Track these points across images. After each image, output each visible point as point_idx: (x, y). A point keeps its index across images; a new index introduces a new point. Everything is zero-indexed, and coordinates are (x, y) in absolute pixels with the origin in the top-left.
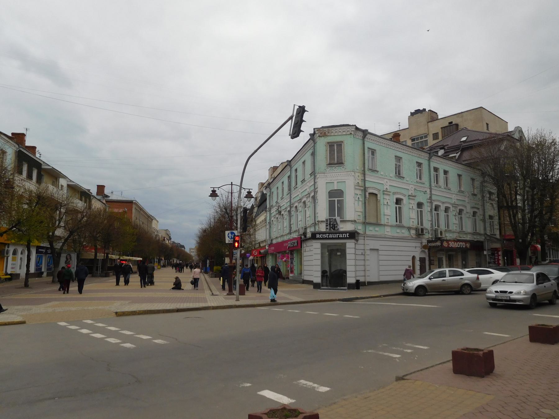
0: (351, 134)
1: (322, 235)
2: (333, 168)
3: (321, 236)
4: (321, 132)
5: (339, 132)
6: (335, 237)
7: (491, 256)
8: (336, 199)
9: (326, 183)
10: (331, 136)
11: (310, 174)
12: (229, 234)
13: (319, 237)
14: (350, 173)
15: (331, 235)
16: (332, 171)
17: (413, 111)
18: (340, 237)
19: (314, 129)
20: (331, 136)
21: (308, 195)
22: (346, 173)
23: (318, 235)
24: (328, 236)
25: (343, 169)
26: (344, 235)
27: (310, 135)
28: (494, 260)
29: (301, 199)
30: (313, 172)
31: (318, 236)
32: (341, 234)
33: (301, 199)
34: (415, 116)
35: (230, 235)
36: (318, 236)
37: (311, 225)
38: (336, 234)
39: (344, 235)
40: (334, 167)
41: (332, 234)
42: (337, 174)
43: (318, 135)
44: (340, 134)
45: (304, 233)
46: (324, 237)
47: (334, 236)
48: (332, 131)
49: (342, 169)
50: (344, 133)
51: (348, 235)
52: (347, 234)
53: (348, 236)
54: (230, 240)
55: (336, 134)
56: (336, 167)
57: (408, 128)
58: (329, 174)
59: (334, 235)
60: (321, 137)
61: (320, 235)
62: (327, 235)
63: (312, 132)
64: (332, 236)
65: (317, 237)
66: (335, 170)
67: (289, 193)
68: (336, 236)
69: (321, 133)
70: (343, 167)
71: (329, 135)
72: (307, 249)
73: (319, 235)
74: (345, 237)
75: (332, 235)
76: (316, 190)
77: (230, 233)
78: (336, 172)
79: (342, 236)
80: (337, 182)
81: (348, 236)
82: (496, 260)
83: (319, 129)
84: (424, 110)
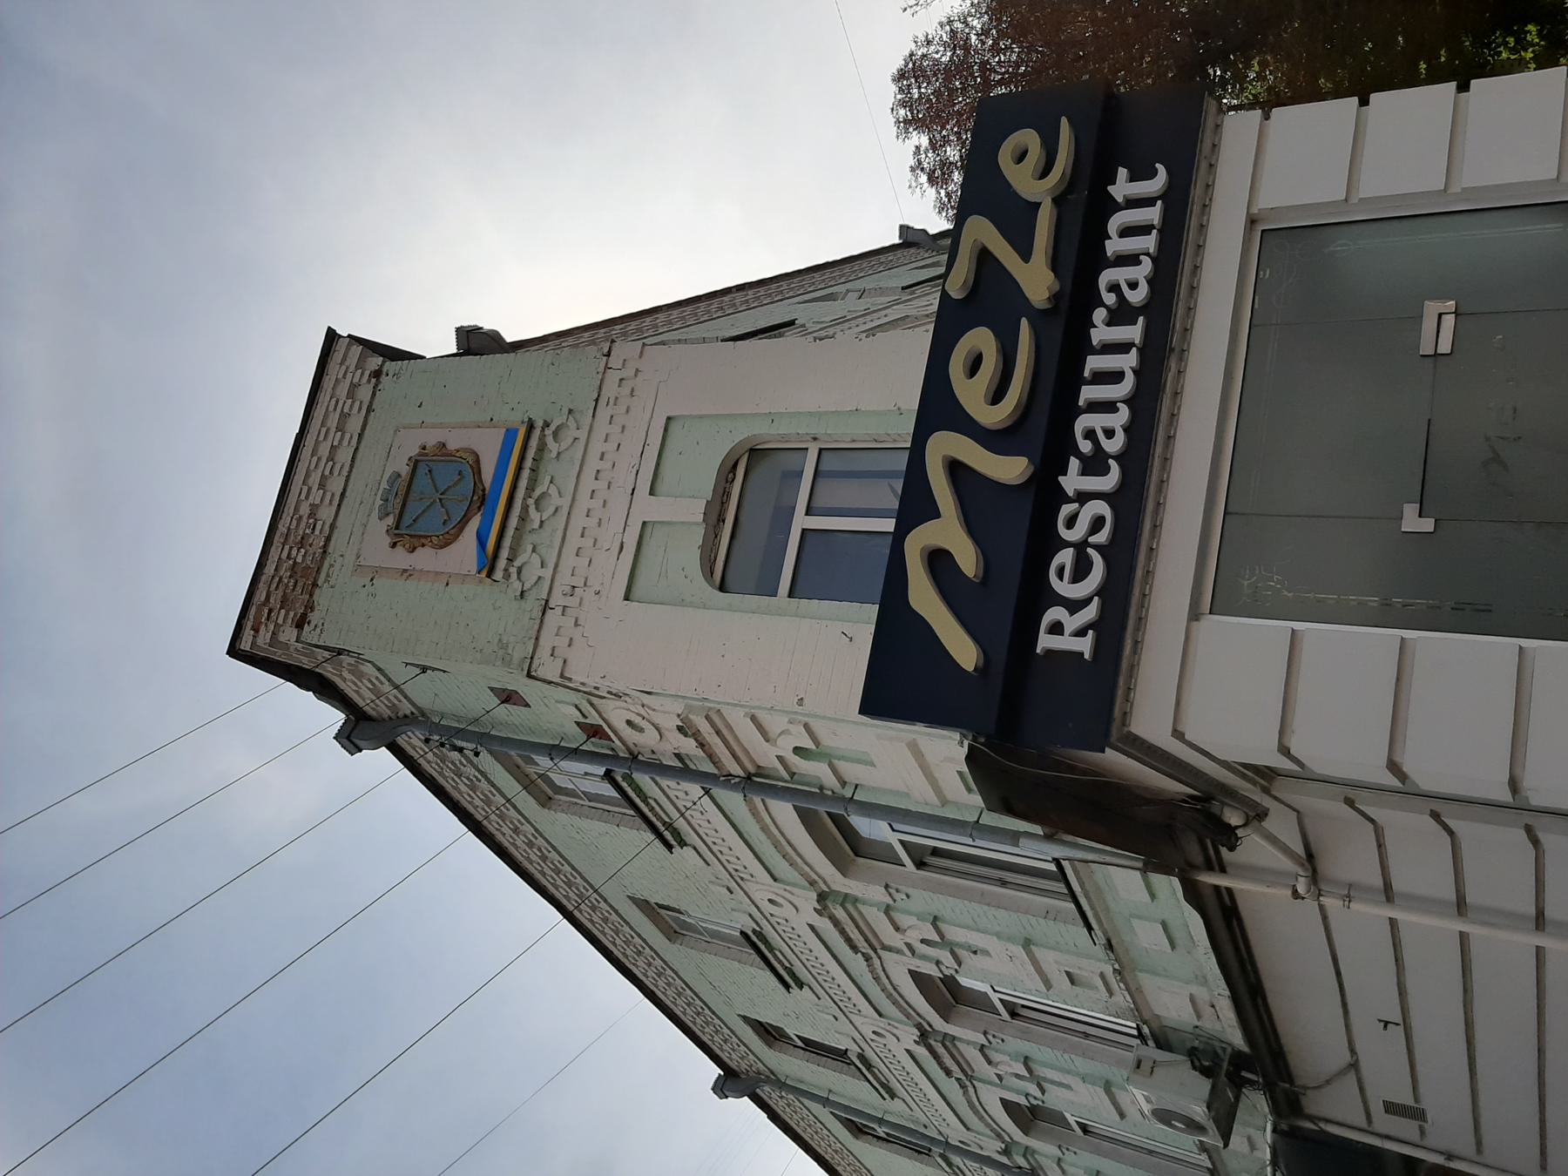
0: (377, 374)
1: (1065, 557)
2: (534, 515)
3: (1081, 571)
4: (275, 601)
5: (331, 458)
6: (1128, 362)
8: (801, 521)
9: (627, 598)
10: (332, 527)
11: (669, 847)
13: (1090, 613)
14: (612, 378)
15: (1083, 422)
16: (554, 531)
18: (1137, 297)
19: (234, 651)
20: (332, 527)
22: (604, 413)
24: (1095, 464)
26: (1126, 232)
27: (351, 739)
29: (919, 1027)
30: (608, 776)
31: (1072, 622)
36: (1072, 622)
37: (1101, 940)
38: (1077, 344)
39: (1126, 232)
40: (532, 509)
41: (1067, 409)
42: (588, 482)
43: (289, 635)
44: (344, 456)
45: (1206, 1072)
46: (1097, 524)
47: (1116, 377)
48: (305, 510)
49: (564, 445)
50: (354, 425)
51: (1133, 178)
52: (1122, 188)
53: (1156, 184)
55: (336, 485)
58: (569, 560)
59: (1103, 377)
60: (310, 607)
61: (1064, 588)
62: (1072, 481)
63: (335, 718)
64: (1109, 407)
65: (1085, 645)
66: (555, 500)
67: (941, 1156)
68: (1122, 348)
69: (284, 602)
70: (555, 434)
71: (322, 544)
72: (1388, 1081)
73: (1055, 613)
74: (1153, 214)
78: (565, 502)
79: (1132, 260)
80: (652, 493)
81: (1156, 184)
83: (253, 610)
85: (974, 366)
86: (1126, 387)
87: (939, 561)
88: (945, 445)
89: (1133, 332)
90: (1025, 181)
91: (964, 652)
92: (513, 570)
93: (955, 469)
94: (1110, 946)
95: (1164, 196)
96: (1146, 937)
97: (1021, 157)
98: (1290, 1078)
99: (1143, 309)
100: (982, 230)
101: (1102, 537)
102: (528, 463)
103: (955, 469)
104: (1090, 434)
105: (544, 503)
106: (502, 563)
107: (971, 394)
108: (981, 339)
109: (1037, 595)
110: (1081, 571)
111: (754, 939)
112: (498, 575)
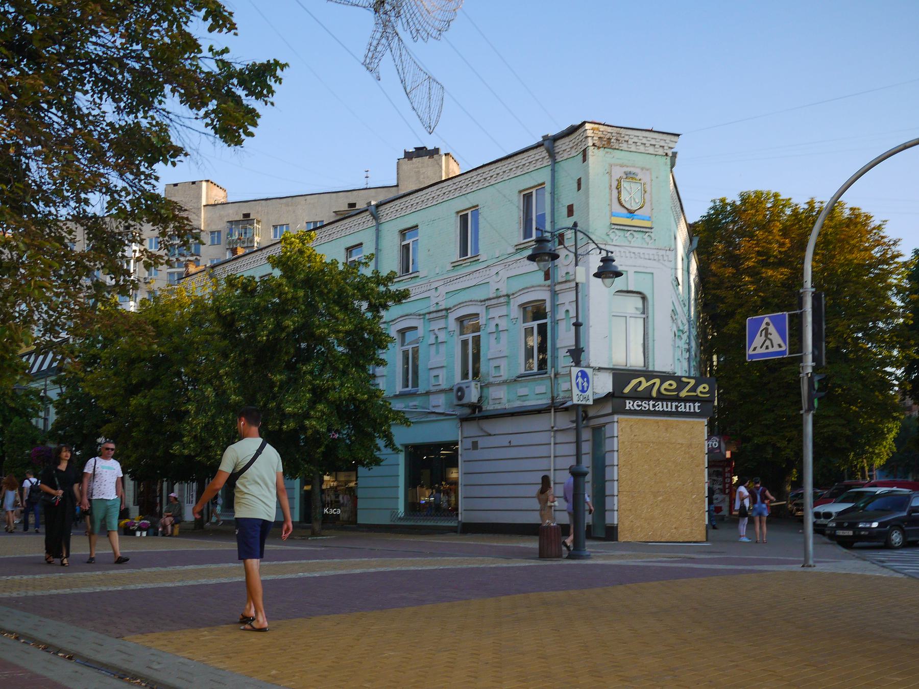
1: (640, 403)
3: (638, 406)
6: (669, 409)
7: (715, 478)
12: (577, 377)
13: (632, 408)
14: (663, 252)
15: (660, 403)
17: (411, 150)
18: (679, 409)
21: (502, 300)
22: (655, 252)
23: (630, 403)
24: (654, 406)
25: (650, 242)
26: (690, 406)
28: (721, 487)
29: (450, 309)
32: (683, 404)
33: (447, 310)
34: (414, 160)
35: (580, 380)
39: (690, 406)
40: (629, 232)
45: (478, 401)
46: (645, 408)
47: (667, 408)
52: (697, 404)
54: (580, 393)
56: (634, 233)
57: (397, 186)
59: (667, 405)
62: (651, 403)
64: (662, 407)
65: (627, 408)
68: (671, 408)
73: (632, 403)
75: (663, 405)
76: (558, 288)
77: (580, 374)
79: (685, 408)
81: (697, 411)
82: (727, 486)
84: (436, 151)
85: (671, 385)
86: (666, 410)
87: (640, 383)
88: (657, 381)
89: (674, 410)
90: (700, 389)
91: (627, 390)
92: (614, 230)
93: (654, 383)
94: (515, 380)
95: (695, 412)
96: (522, 390)
97: (704, 388)
98: (479, 419)
99: (677, 411)
100: (693, 382)
101: (643, 409)
102: (642, 230)
103: (654, 383)
104: (658, 405)
105: (631, 236)
106: (616, 227)
107: (666, 385)
108: (675, 385)
109: (634, 399)
110: (638, 406)
111: (476, 258)
112: (613, 227)
